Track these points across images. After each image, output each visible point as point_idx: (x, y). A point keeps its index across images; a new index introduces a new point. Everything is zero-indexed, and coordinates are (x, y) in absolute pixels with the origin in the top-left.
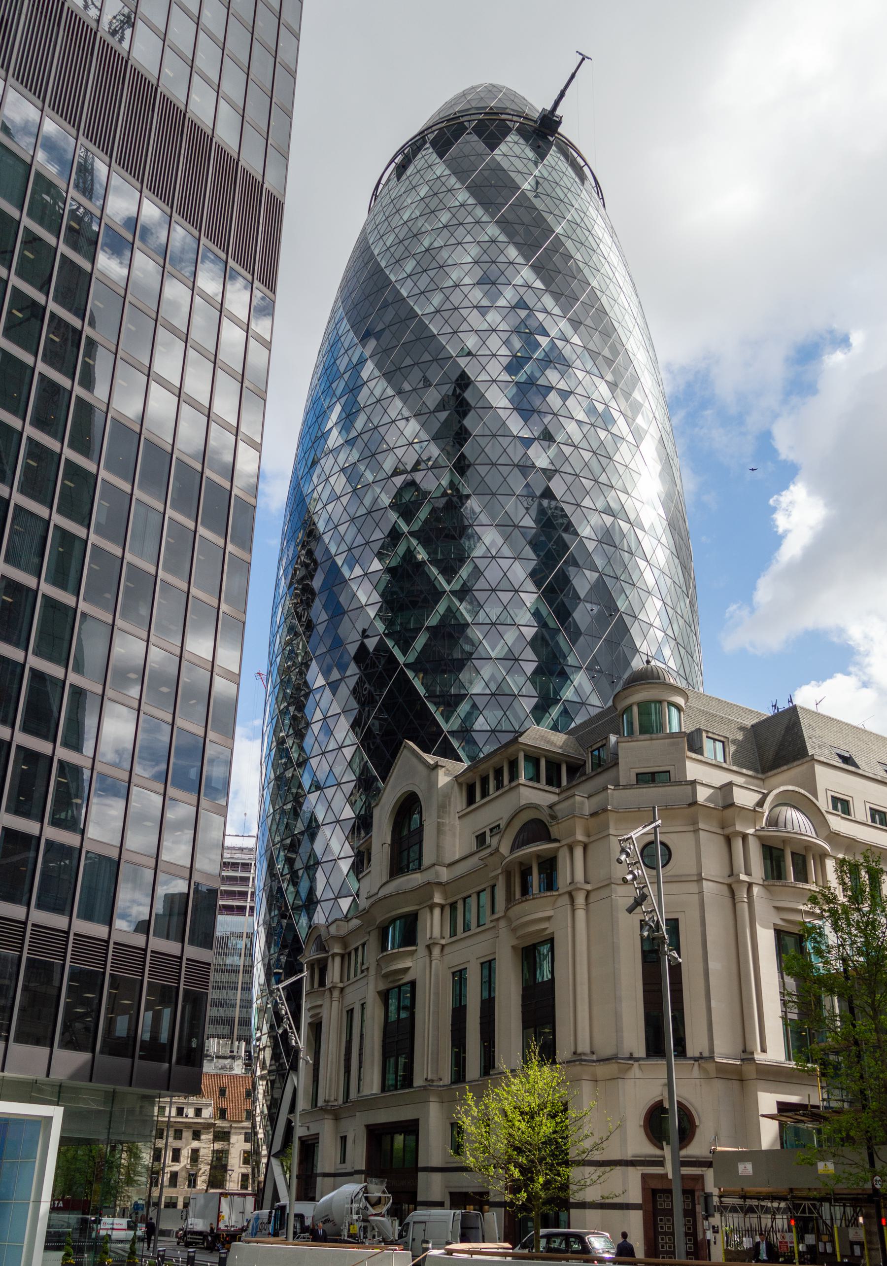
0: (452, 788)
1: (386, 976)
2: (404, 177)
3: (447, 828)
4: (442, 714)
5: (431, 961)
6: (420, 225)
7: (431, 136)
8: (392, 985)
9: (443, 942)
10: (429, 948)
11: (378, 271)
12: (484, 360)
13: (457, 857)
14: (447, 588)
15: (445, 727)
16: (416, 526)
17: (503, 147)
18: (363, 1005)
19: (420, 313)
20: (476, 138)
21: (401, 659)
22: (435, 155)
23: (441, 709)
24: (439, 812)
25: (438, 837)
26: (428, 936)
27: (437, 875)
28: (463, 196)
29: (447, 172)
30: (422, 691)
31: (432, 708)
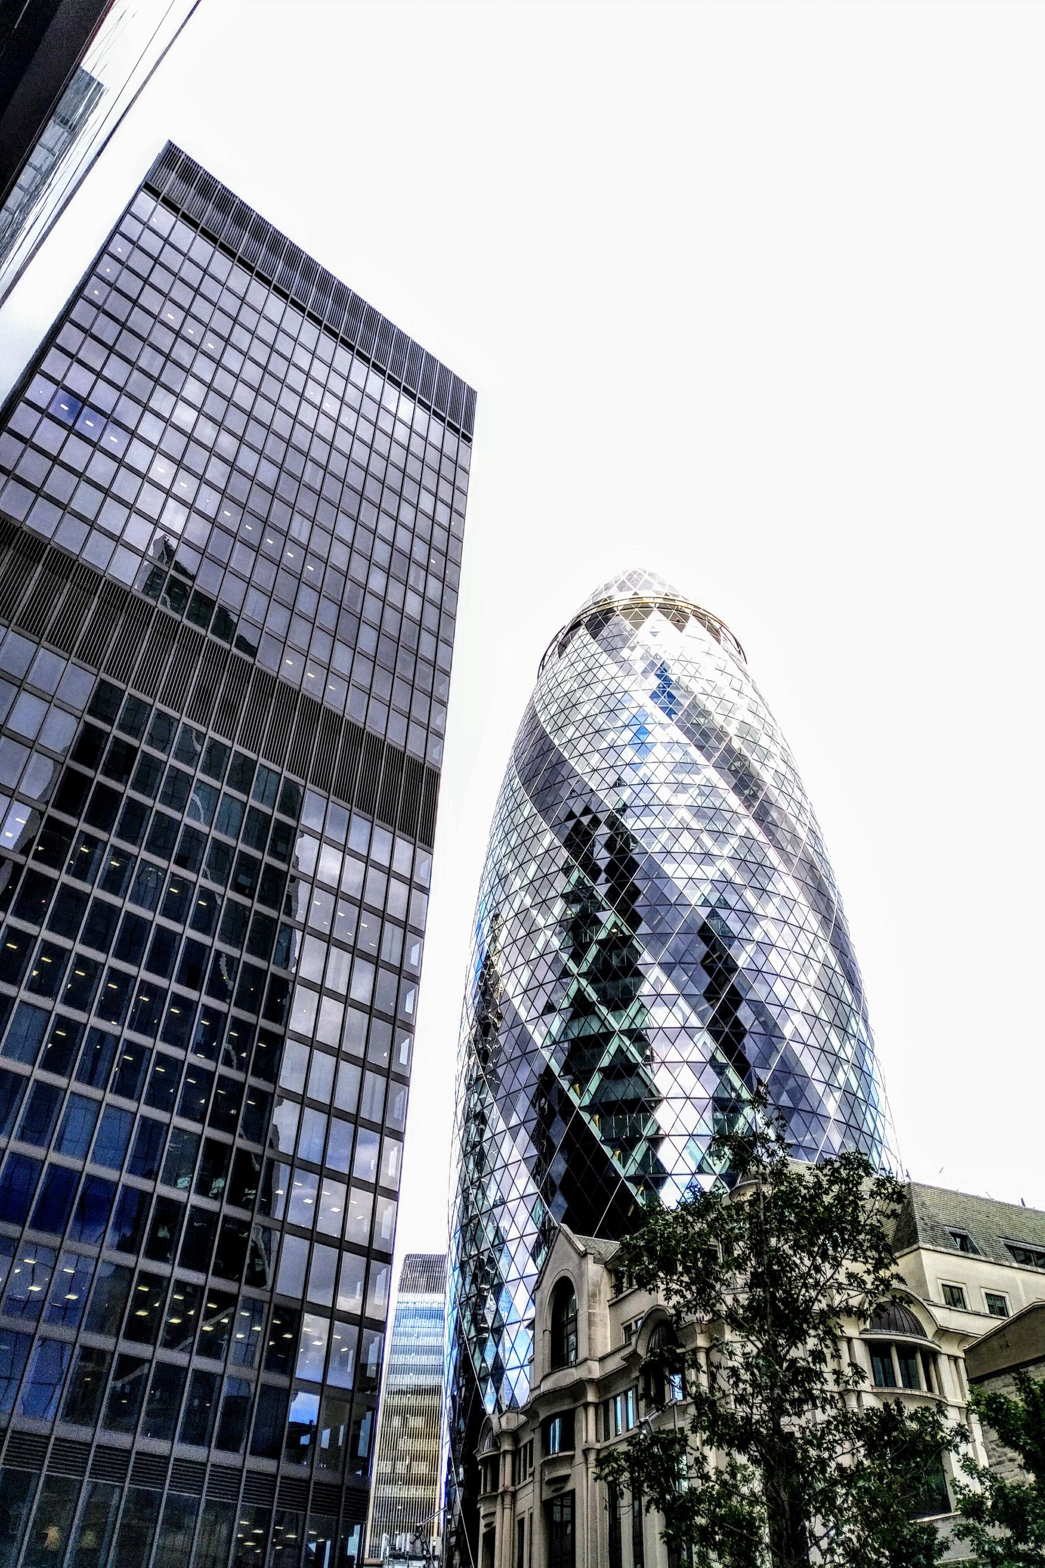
1: (550, 1482)
2: (564, 655)
3: (597, 1319)
4: (619, 1159)
8: (555, 1494)
9: (598, 1446)
10: (586, 1452)
11: (544, 736)
13: (609, 1350)
14: (617, 1027)
15: (622, 1172)
16: (584, 968)
18: (531, 1515)
19: (580, 772)
22: (589, 636)
23: (618, 1153)
26: (584, 1439)
27: (590, 1371)
29: (600, 650)
31: (607, 1150)
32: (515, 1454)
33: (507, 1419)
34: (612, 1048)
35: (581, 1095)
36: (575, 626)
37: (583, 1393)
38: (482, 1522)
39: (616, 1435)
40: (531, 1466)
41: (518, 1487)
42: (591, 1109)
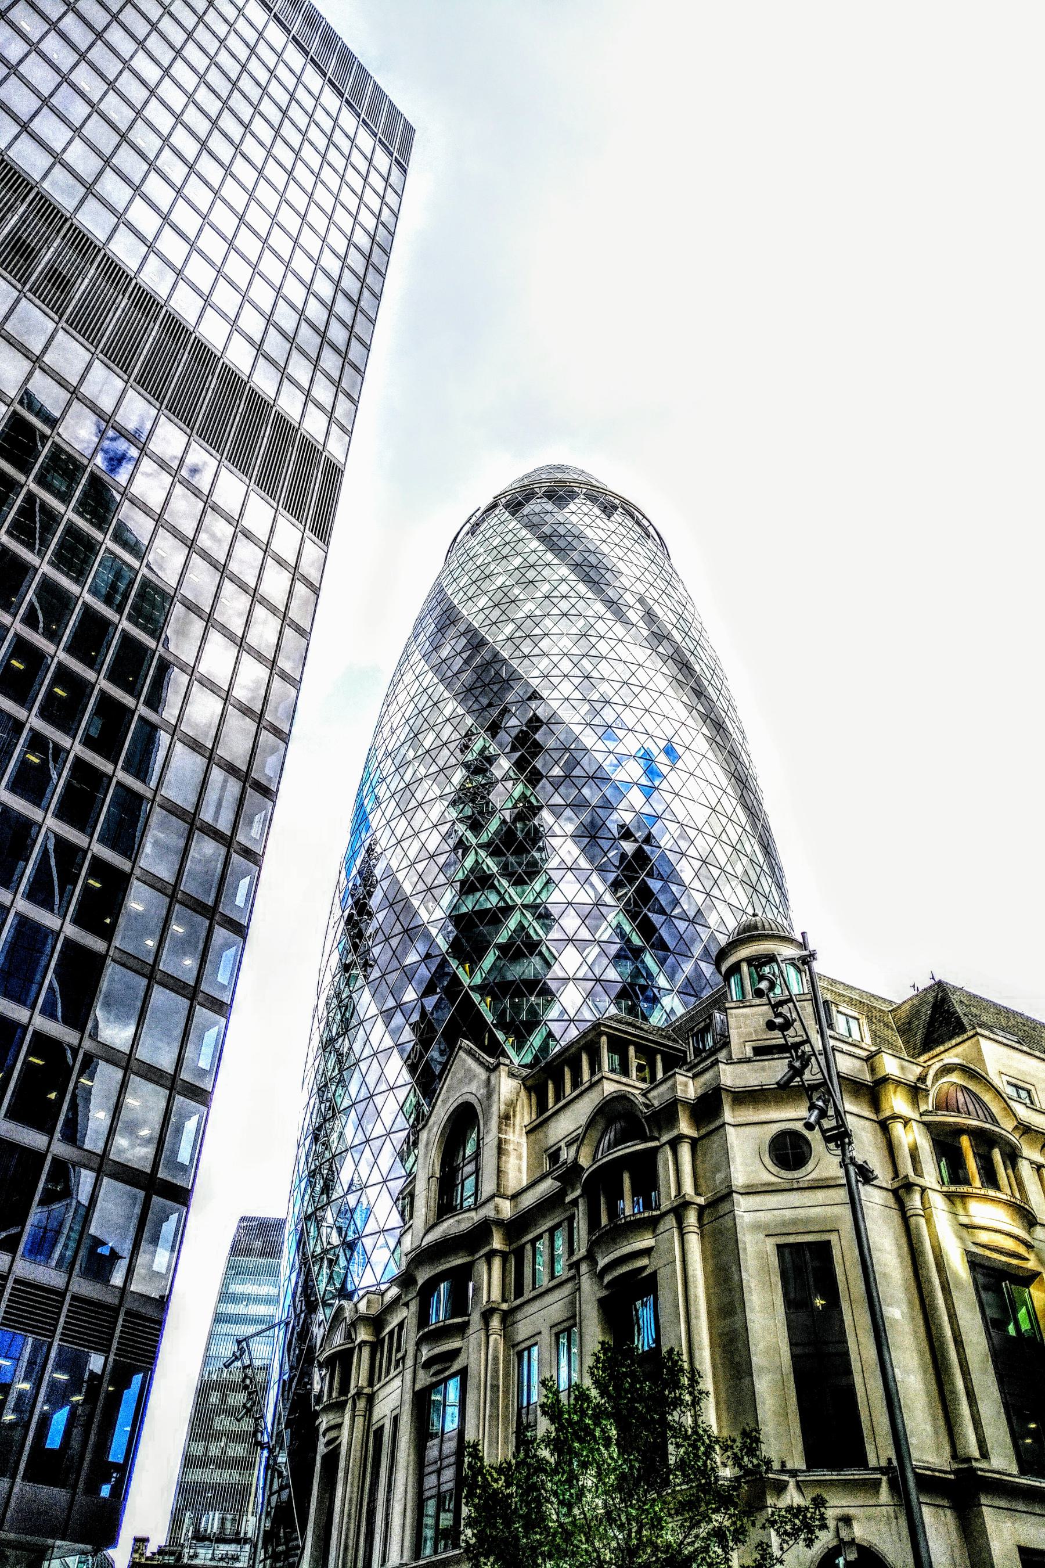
0: (518, 1094)
3: (510, 1147)
5: (488, 1336)
6: (492, 568)
7: (504, 500)
9: (505, 1306)
12: (555, 681)
13: (524, 1183)
17: (572, 507)
19: (491, 641)
20: (545, 500)
21: (465, 980)
22: (507, 514)
24: (500, 1123)
25: (499, 1158)
26: (485, 1299)
27: (497, 1209)
28: (535, 544)
30: (489, 1018)
31: (500, 1036)
32: (375, 1347)
33: (368, 1301)
34: (512, 923)
35: (472, 973)
36: (494, 506)
37: (488, 1238)
38: (322, 1441)
39: (534, 1288)
40: (398, 1350)
41: (375, 1388)
42: (482, 989)
